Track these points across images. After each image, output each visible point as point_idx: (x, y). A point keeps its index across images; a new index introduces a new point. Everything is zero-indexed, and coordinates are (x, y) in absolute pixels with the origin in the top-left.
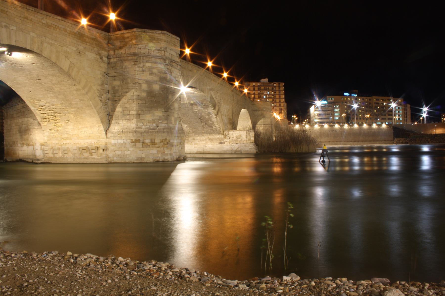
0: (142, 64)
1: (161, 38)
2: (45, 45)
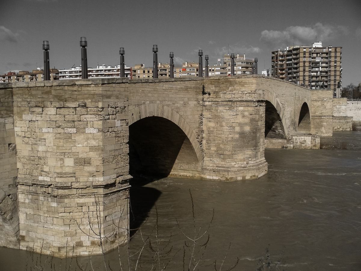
0: (235, 109)
1: (251, 81)
2: (165, 107)
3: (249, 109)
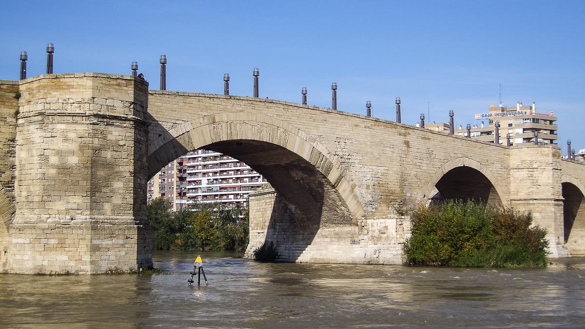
1: (84, 84)
3: (78, 127)
